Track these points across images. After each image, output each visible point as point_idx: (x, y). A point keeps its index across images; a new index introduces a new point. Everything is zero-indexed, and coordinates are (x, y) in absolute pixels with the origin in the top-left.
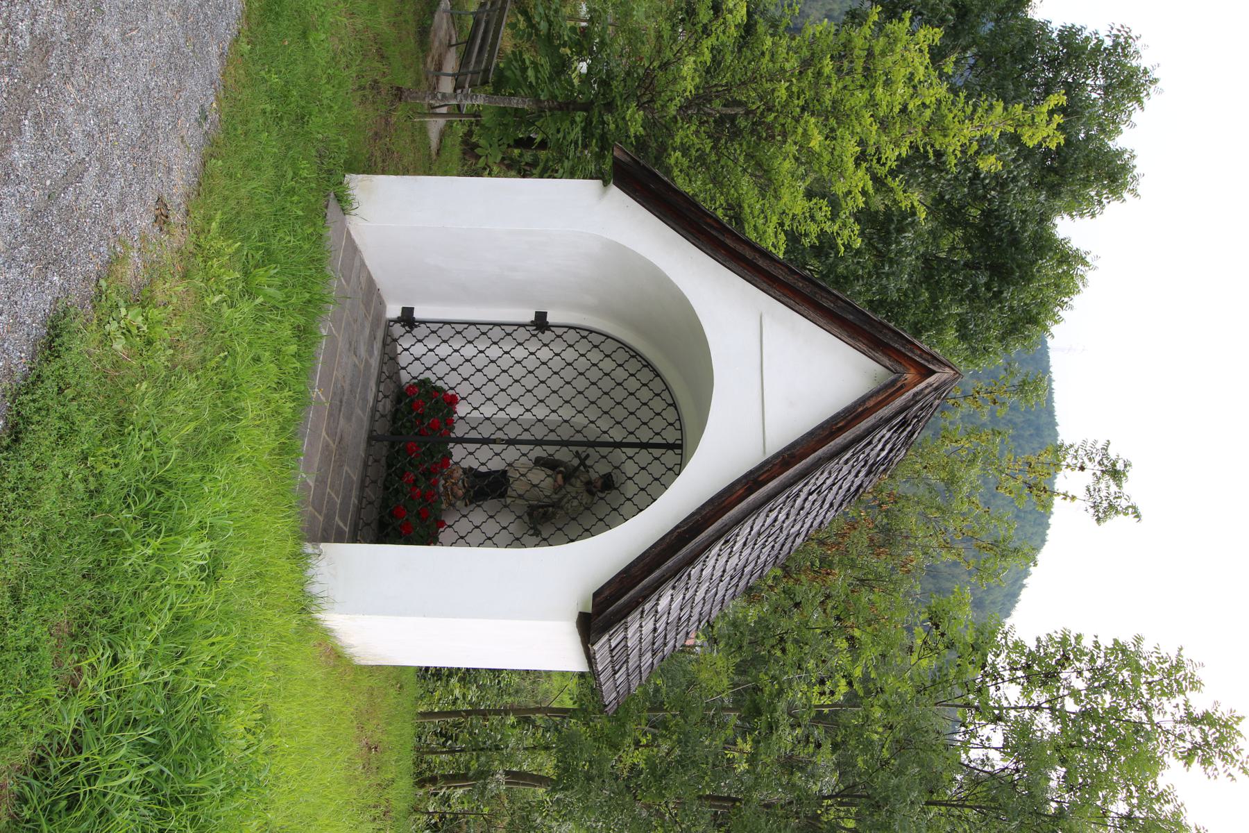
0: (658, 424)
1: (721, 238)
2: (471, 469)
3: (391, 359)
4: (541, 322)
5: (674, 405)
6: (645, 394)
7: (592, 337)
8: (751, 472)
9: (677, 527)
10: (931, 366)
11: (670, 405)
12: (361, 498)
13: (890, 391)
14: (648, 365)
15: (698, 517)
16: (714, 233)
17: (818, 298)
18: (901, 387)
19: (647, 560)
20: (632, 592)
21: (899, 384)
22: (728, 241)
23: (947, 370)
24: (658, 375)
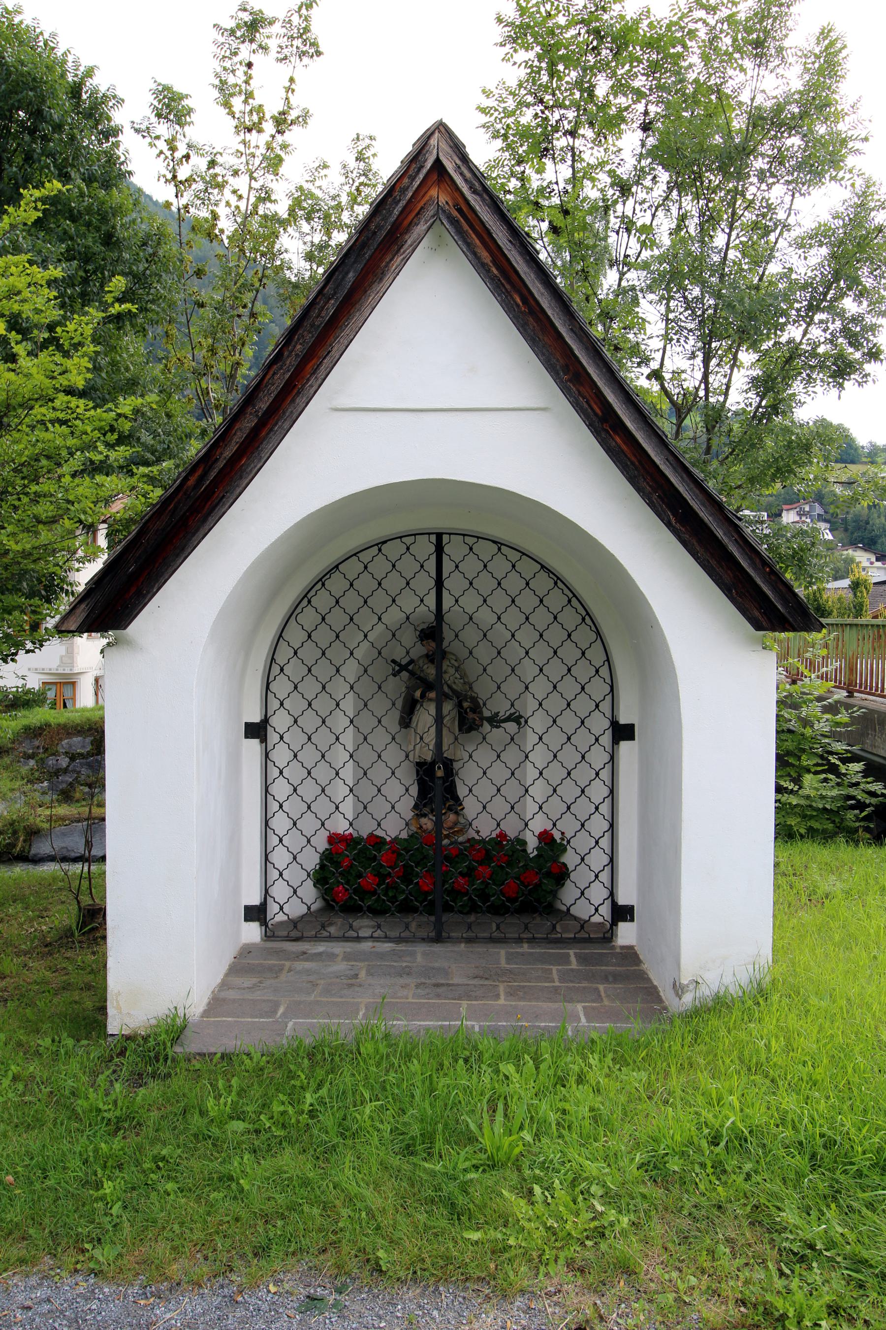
0: (408, 566)
1: (221, 464)
2: (416, 807)
3: (295, 927)
4: (256, 731)
5: (380, 544)
6: (365, 584)
7: (281, 659)
8: (590, 426)
9: (668, 525)
10: (429, 165)
11: (380, 550)
12: (519, 940)
13: (466, 227)
14: (321, 581)
15: (655, 497)
16: (213, 474)
17: (321, 322)
18: (460, 210)
19: (713, 563)
20: (758, 581)
21: (455, 214)
22: (228, 453)
23: (433, 141)
24: (337, 567)
